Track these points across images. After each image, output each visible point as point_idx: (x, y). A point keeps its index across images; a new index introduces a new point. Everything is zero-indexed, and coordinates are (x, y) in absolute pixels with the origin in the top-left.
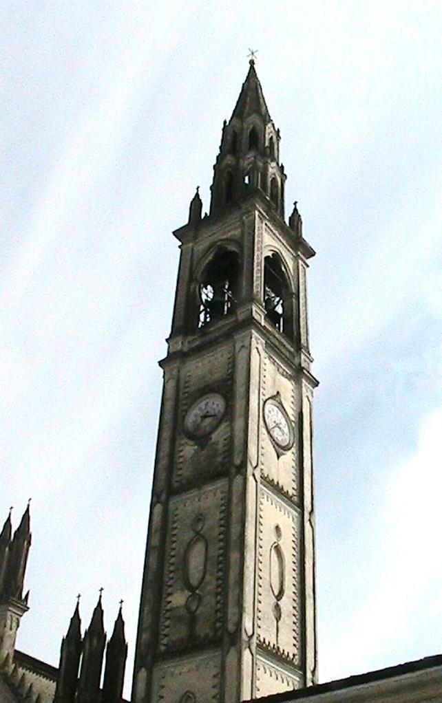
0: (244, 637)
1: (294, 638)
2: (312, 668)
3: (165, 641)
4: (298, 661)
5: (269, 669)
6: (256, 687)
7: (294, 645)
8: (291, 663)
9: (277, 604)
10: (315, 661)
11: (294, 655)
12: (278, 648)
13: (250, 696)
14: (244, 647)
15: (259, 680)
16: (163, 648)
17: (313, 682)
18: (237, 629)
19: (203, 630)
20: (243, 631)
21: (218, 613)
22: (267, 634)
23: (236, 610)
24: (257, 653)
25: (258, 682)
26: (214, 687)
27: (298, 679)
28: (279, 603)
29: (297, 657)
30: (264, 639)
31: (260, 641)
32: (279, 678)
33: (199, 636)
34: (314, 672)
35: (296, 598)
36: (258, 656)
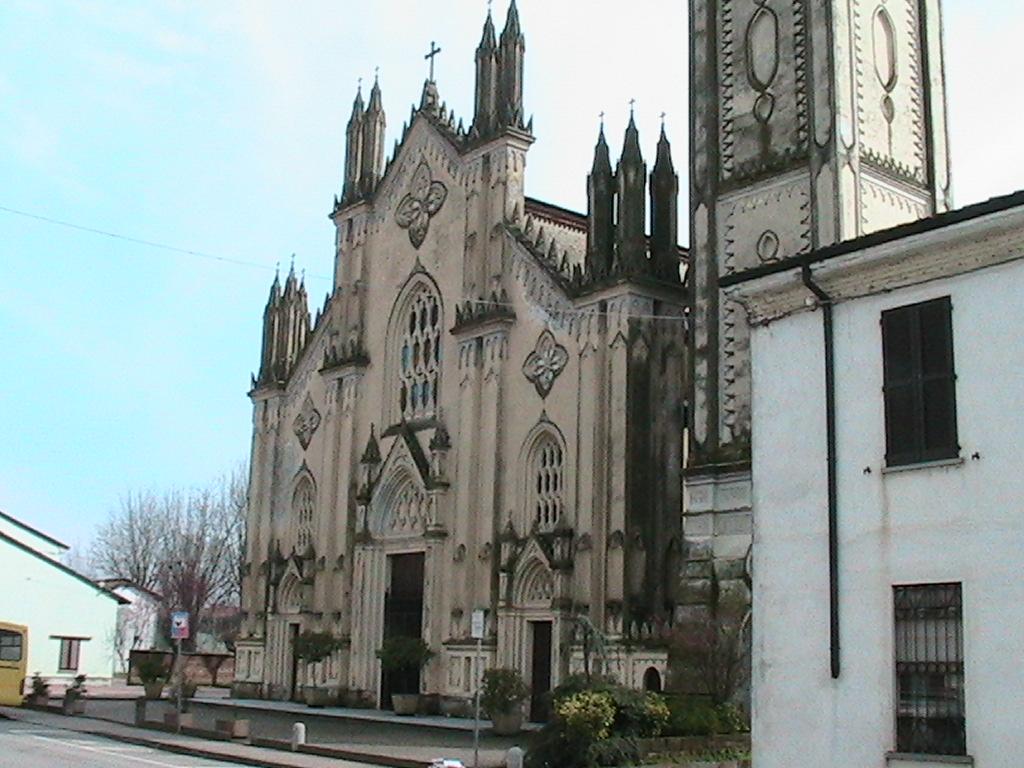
0: (841, 150)
1: (916, 144)
2: (944, 186)
3: (729, 165)
4: (922, 177)
5: (889, 194)
6: (862, 217)
7: (916, 155)
8: (912, 180)
9: (888, 98)
10: (948, 176)
11: (916, 169)
12: (892, 160)
13: (854, 232)
14: (840, 164)
15: (866, 207)
16: (727, 175)
17: (946, 205)
18: (830, 138)
19: (781, 144)
20: (839, 142)
21: (801, 118)
22: (875, 142)
23: (827, 111)
24: (861, 171)
25: (864, 211)
26: (802, 222)
27: (923, 202)
28: (890, 95)
29: (920, 171)
30: (871, 150)
31: (864, 153)
32: (896, 201)
33: (776, 154)
34: (946, 190)
35: (915, 86)
36: (863, 175)
